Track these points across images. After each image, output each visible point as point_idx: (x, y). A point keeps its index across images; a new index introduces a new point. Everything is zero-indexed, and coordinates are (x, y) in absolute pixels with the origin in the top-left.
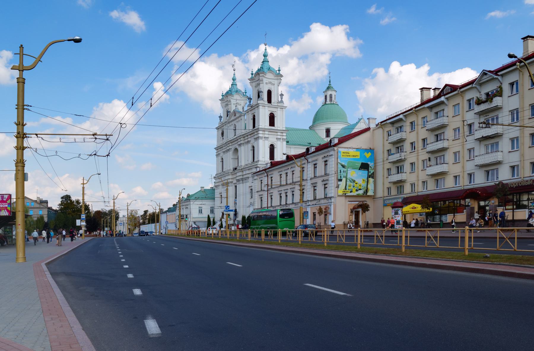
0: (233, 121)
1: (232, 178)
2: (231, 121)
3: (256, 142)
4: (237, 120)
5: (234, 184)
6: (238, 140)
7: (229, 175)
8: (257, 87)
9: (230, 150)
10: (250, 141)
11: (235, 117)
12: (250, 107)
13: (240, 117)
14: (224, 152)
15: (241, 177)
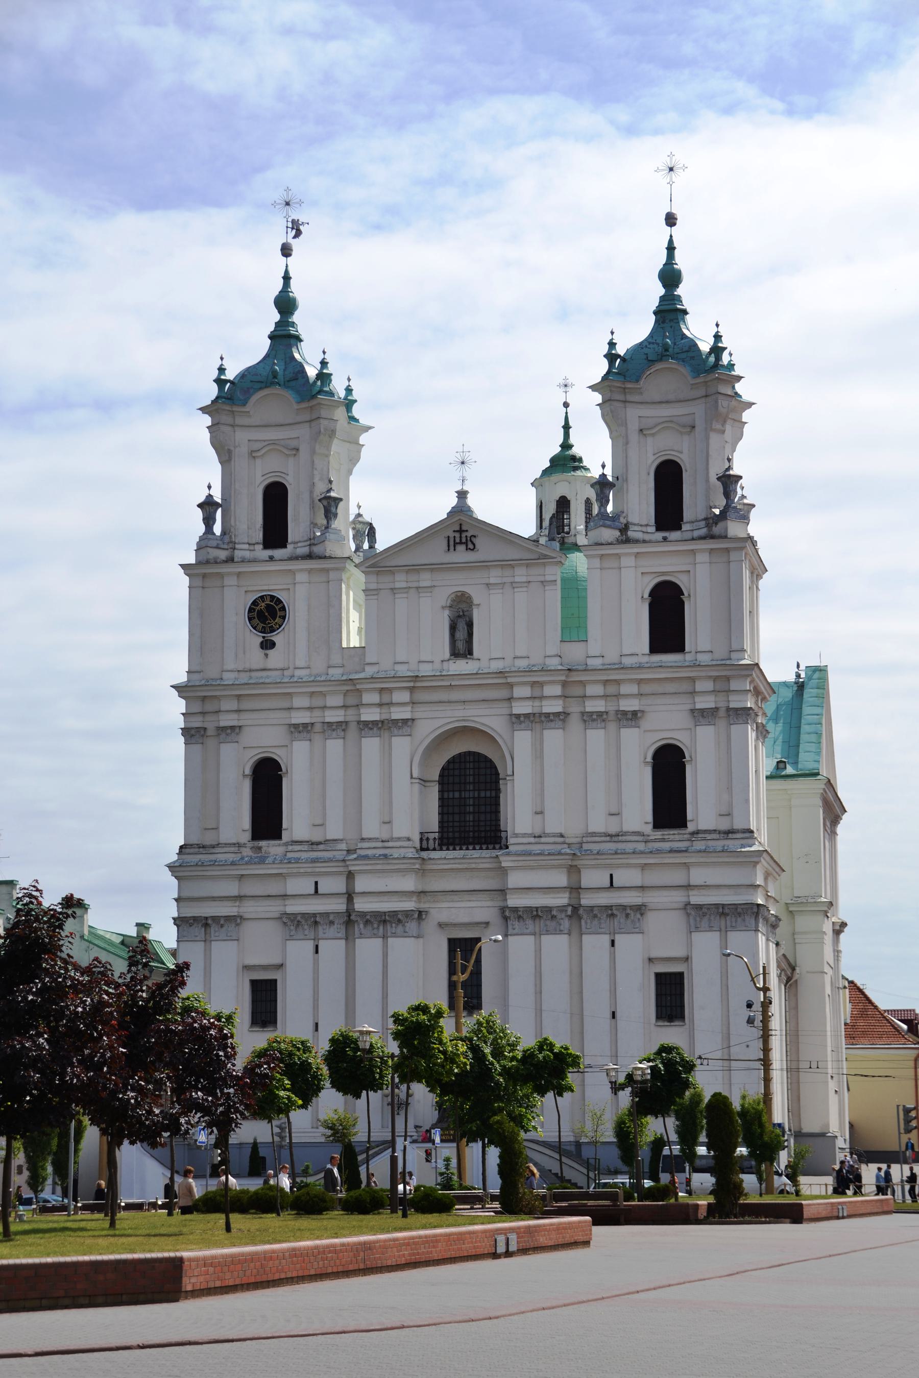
0: (432, 570)
1: (420, 890)
2: (414, 569)
3: (711, 728)
4: (494, 576)
5: (441, 925)
6: (511, 686)
7: (413, 870)
8: (653, 435)
9: (406, 730)
10: (643, 712)
11: (461, 555)
12: (617, 533)
13: (527, 566)
14: (301, 730)
15: (562, 900)
